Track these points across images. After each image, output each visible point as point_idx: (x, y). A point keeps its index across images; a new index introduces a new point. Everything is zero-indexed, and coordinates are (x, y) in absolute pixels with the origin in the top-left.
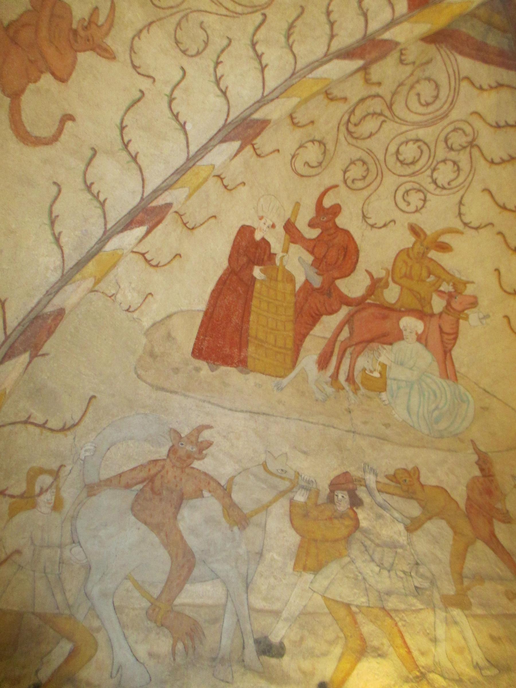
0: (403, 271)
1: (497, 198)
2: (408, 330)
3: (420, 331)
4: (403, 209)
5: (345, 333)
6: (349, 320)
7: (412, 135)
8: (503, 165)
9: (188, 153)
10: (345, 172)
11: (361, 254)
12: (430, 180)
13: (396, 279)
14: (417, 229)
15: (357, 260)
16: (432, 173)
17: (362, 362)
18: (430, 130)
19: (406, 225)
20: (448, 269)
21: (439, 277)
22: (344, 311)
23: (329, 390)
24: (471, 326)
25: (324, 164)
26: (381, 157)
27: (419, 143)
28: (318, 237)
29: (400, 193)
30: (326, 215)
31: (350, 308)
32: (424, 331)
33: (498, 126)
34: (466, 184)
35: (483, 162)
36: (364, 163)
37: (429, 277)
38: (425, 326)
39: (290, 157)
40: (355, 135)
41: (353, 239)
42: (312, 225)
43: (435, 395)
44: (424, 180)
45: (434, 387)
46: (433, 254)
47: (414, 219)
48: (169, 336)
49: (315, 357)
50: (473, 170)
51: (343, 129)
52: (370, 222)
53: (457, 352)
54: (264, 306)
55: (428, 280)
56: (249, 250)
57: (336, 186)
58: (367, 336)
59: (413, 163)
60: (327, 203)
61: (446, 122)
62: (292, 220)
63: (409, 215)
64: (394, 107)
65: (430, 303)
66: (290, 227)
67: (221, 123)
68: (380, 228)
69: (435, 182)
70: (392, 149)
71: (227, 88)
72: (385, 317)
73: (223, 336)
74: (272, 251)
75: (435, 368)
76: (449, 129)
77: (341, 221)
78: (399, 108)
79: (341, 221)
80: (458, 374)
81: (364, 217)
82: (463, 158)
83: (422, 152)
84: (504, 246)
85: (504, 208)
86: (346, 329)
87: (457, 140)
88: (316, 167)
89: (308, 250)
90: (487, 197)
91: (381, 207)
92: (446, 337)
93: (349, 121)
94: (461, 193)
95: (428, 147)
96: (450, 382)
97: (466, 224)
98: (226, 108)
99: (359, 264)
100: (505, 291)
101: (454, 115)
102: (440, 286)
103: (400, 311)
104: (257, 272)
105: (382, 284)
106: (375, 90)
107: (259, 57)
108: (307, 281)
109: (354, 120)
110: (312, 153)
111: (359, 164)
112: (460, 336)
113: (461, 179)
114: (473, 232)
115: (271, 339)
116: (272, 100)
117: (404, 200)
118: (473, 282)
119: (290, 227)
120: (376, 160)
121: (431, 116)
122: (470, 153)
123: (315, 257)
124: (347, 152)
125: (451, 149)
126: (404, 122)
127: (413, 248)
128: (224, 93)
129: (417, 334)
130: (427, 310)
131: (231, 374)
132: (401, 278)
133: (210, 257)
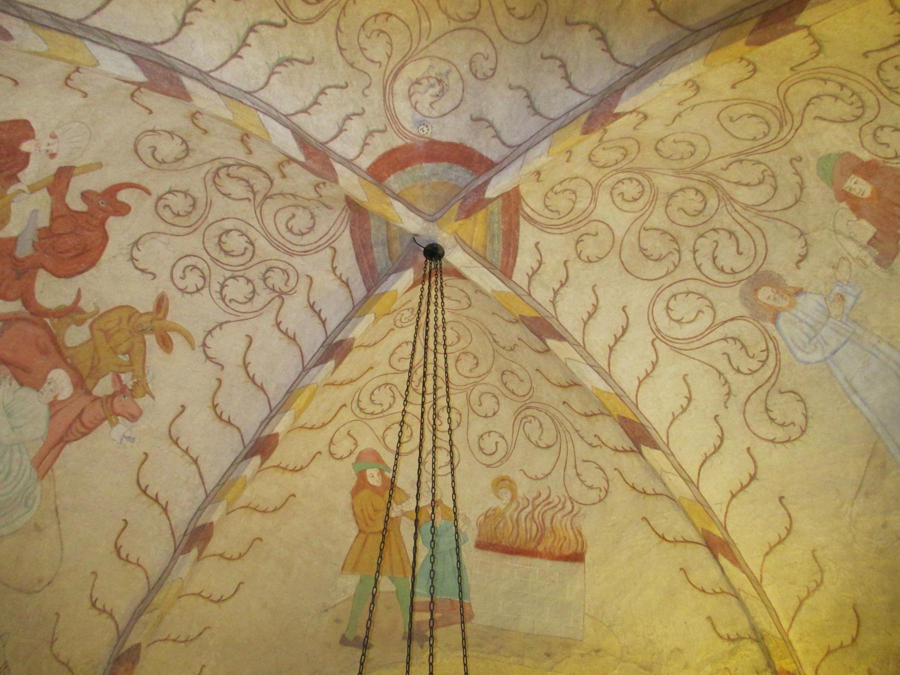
0: (110, 326)
1: (249, 352)
2: (51, 387)
3: (60, 398)
4: (174, 276)
7: (253, 235)
8: (282, 336)
9: (87, 17)
10: (170, 192)
11: (93, 271)
12: (221, 280)
13: (95, 326)
14: (164, 306)
15: (82, 272)
16: (230, 278)
18: (271, 248)
19: (160, 291)
20: (147, 364)
21: (131, 363)
24: (109, 437)
25: (164, 166)
26: (211, 219)
27: (250, 247)
28: (77, 212)
30: (109, 203)
31: (23, 309)
32: (63, 401)
33: (312, 307)
34: (243, 316)
35: (273, 316)
36: (194, 206)
37: (124, 354)
38: (72, 396)
39: (151, 128)
40: (217, 180)
41: (103, 250)
42: (85, 196)
44: (218, 275)
45: (15, 467)
47: (173, 294)
50: (256, 314)
51: (217, 164)
52: (136, 254)
55: (121, 357)
57: (149, 193)
59: (226, 253)
60: (123, 196)
61: (286, 257)
62: (76, 171)
63: (173, 287)
64: (269, 201)
65: (98, 379)
66: (64, 174)
67: (150, 39)
68: (136, 268)
69: (223, 286)
70: (228, 225)
71: (191, 23)
72: (45, 352)
74: (20, 175)
76: (282, 265)
77: (114, 224)
78: (270, 207)
79: (114, 224)
80: (50, 472)
81: (136, 243)
82: (264, 296)
83: (243, 254)
84: (211, 394)
85: (246, 366)
87: (276, 279)
88: (157, 160)
89: (52, 213)
90: (244, 344)
92: (78, 424)
93: (228, 166)
94: (232, 318)
95: (252, 257)
96: (35, 475)
97: (204, 345)
98: (168, 35)
99: (80, 277)
100: (170, 431)
101: (297, 261)
102: (124, 372)
103: (64, 359)
105: (78, 317)
106: (276, 175)
107: (244, 43)
108: (14, 240)
109: (233, 171)
111: (190, 201)
112: (90, 436)
113: (243, 308)
114: (203, 357)
116: (213, 89)
117: (184, 271)
118: (153, 397)
119: (64, 174)
120: (204, 216)
121: (282, 241)
122: (273, 299)
123: (51, 227)
124: (194, 182)
125: (265, 280)
126: (261, 221)
127: (141, 315)
128: (183, 24)
129: (56, 397)
130: (89, 383)
132: (101, 330)
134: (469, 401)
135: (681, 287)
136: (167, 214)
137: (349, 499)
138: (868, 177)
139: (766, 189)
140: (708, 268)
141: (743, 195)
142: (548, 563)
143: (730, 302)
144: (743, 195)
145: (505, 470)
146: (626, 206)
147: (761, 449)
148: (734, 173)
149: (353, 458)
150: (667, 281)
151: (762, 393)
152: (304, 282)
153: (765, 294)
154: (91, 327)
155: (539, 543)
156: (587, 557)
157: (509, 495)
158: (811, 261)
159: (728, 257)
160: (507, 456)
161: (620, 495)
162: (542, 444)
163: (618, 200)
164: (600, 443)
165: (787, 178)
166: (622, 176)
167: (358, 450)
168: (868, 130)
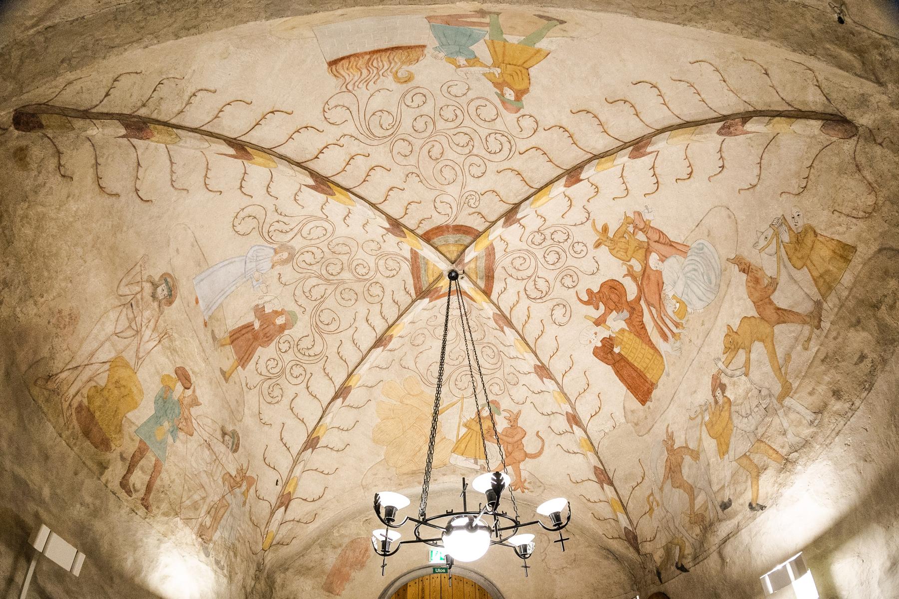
5: (654, 311)
6: (649, 304)
17: (670, 311)
22: (642, 302)
29: (576, 255)
30: (592, 299)
43: (695, 270)
44: (566, 246)
46: (611, 235)
47: (590, 246)
49: (661, 340)
51: (544, 299)
53: (672, 235)
54: (632, 355)
56: (606, 351)
58: (657, 297)
60: (585, 298)
61: (530, 249)
66: (598, 322)
73: (640, 386)
77: (596, 290)
78: (529, 272)
79: (596, 290)
86: (652, 308)
91: (587, 265)
109: (539, 295)
110: (559, 313)
115: (647, 361)
119: (598, 322)
130: (646, 245)
134: (434, 124)
135: (322, 239)
136: (575, 278)
137: (531, 88)
138: (280, 326)
139: (307, 290)
140: (314, 250)
141: (314, 281)
142: (359, 50)
143: (298, 243)
144: (314, 281)
146: (360, 262)
147: (246, 201)
148: (321, 289)
149: (522, 112)
150: (330, 239)
151: (261, 221)
152: (524, 239)
153: (285, 255)
154: (629, 261)
155: (369, 59)
156: (326, 66)
157: (399, 74)
158: (276, 280)
159: (308, 258)
160: (404, 96)
161: (314, 117)
163: (365, 265)
164: (338, 143)
165: (302, 301)
166: (367, 277)
167: (518, 115)
168: (292, 343)
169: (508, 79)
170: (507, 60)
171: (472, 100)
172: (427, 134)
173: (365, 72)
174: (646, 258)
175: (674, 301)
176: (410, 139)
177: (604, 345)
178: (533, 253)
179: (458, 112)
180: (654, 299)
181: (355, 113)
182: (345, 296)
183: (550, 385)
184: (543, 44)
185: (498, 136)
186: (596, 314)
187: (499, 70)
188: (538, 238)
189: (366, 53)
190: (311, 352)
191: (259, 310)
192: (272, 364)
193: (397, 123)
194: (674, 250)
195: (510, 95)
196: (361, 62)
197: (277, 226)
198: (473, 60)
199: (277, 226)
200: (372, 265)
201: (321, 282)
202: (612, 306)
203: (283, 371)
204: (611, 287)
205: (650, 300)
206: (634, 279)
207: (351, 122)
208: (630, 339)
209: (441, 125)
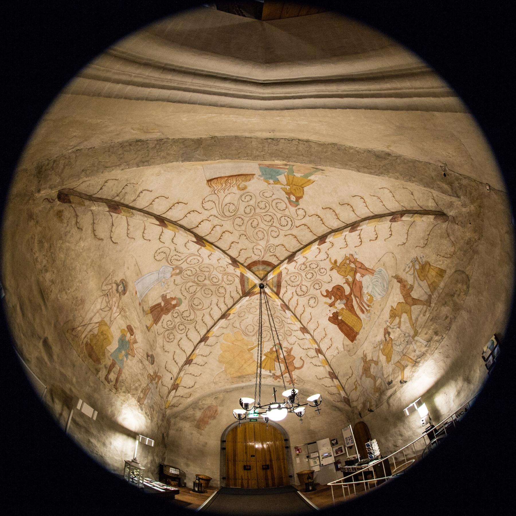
6: (355, 296)
7: (305, 277)
17: (365, 299)
22: (352, 296)
23: (369, 315)
30: (329, 294)
42: (331, 299)
43: (377, 281)
44: (316, 270)
46: (338, 264)
47: (328, 270)
48: (347, 345)
53: (367, 265)
56: (334, 319)
60: (325, 294)
66: (331, 305)
72: (356, 284)
73: (351, 334)
75: (371, 276)
77: (330, 290)
78: (298, 283)
79: (330, 290)
82: (308, 264)
87: (303, 267)
91: (326, 278)
104: (340, 318)
109: (302, 293)
110: (312, 302)
119: (331, 305)
126: (302, 280)
130: (355, 269)
131: (358, 337)
133: (334, 330)
134: (255, 210)
136: (320, 285)
138: (174, 305)
139: (187, 288)
140: (192, 269)
141: (191, 284)
143: (184, 266)
144: (191, 284)
145: (242, 192)
146: (214, 276)
147: (161, 245)
148: (195, 288)
149: (298, 207)
151: (168, 255)
153: (178, 271)
156: (206, 182)
157: (240, 186)
158: (172, 283)
159: (189, 273)
160: (241, 196)
161: (197, 206)
162: (229, 205)
165: (185, 293)
167: (296, 208)
169: (293, 191)
170: (294, 183)
171: (274, 199)
172: (251, 215)
173: (224, 185)
174: (355, 275)
175: (367, 295)
176: (243, 217)
177: (334, 316)
178: (300, 274)
179: (267, 205)
180: (358, 294)
181: (217, 205)
182: (207, 292)
183: (307, 336)
184: (312, 178)
185: (286, 218)
186: (330, 301)
187: (289, 187)
188: (303, 267)
189: (226, 177)
190: (189, 319)
191: (164, 297)
192: (169, 323)
193: (237, 210)
194: (367, 272)
195: (293, 198)
196: (223, 181)
197: (175, 257)
198: (277, 182)
199: (175, 257)
200: (220, 278)
201: (194, 284)
202: (338, 297)
203: (175, 327)
204: (338, 289)
205: (356, 294)
206: (349, 285)
207: (215, 209)
208: (346, 313)
209: (258, 210)
